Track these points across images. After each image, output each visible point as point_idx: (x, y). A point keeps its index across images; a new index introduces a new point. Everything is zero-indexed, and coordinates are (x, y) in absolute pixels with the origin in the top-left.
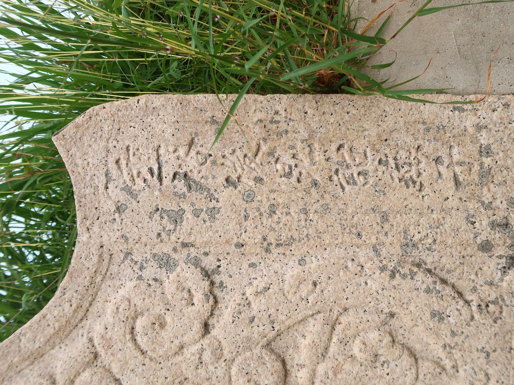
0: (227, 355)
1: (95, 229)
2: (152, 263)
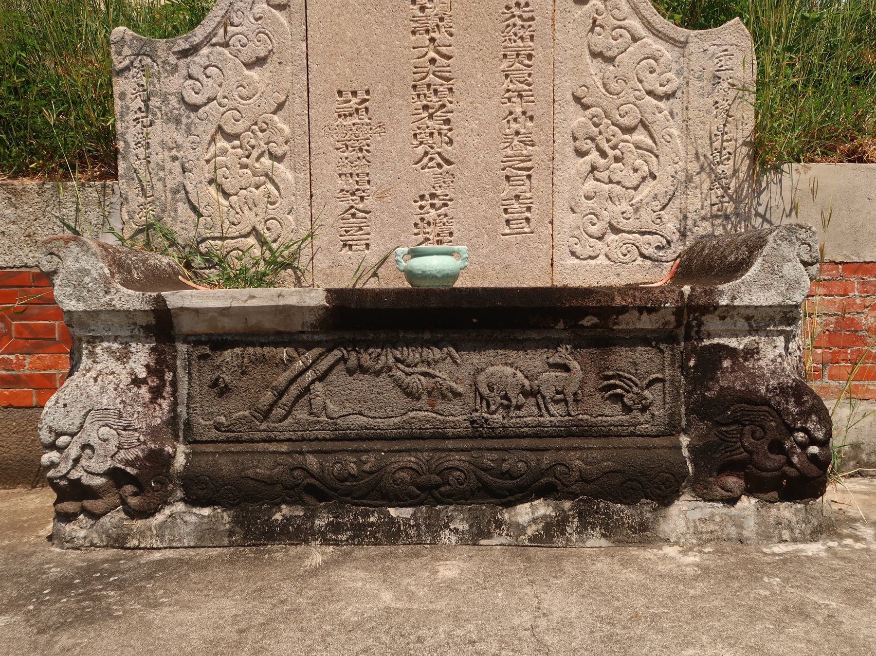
0: (638, 102)
1: (696, 40)
2: (679, 68)
